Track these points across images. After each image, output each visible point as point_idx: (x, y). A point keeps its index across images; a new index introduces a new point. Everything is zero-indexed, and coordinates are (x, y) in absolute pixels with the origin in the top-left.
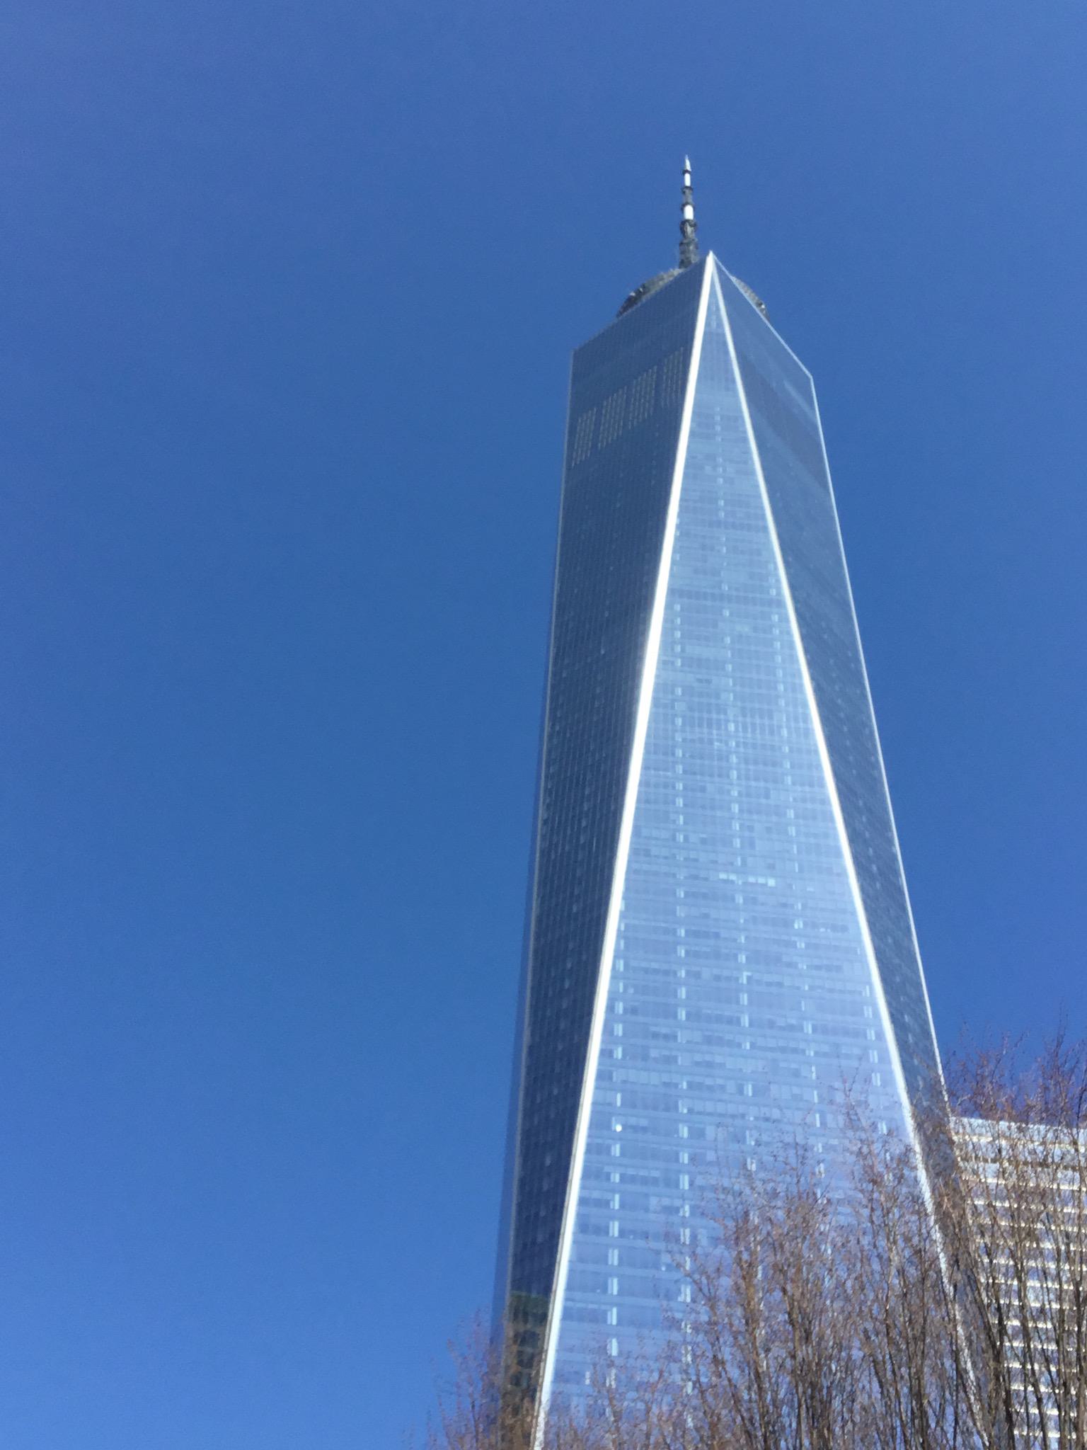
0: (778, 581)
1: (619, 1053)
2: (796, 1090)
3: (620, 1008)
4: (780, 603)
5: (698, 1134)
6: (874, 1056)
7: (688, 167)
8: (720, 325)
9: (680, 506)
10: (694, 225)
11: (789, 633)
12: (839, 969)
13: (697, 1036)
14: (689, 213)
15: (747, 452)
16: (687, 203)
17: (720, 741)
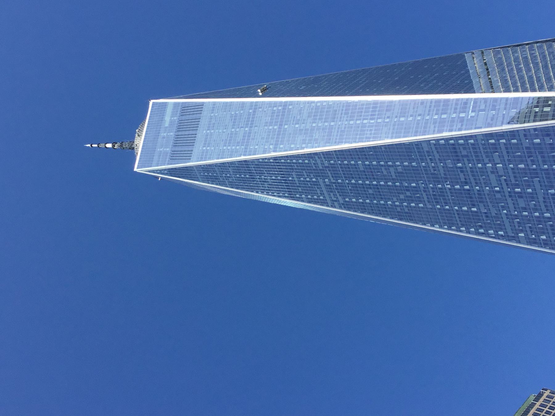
0: (266, 159)
1: (501, 233)
2: (489, 173)
3: (482, 231)
4: (275, 159)
5: (525, 209)
6: (461, 142)
7: (89, 145)
8: (165, 170)
9: (253, 191)
10: (114, 144)
11: (287, 157)
12: (428, 152)
13: (481, 205)
14: (109, 145)
15: (216, 165)
16: (106, 147)
17: (349, 187)
